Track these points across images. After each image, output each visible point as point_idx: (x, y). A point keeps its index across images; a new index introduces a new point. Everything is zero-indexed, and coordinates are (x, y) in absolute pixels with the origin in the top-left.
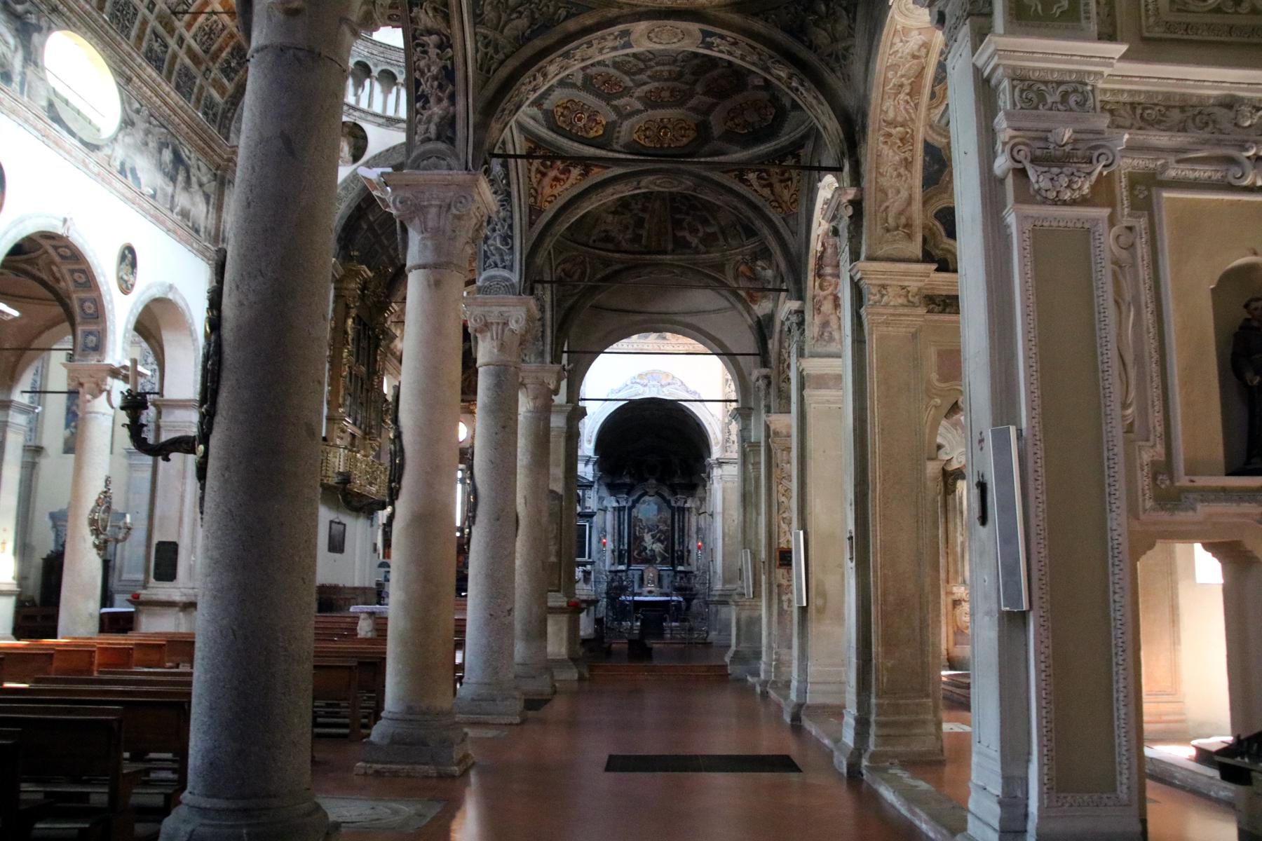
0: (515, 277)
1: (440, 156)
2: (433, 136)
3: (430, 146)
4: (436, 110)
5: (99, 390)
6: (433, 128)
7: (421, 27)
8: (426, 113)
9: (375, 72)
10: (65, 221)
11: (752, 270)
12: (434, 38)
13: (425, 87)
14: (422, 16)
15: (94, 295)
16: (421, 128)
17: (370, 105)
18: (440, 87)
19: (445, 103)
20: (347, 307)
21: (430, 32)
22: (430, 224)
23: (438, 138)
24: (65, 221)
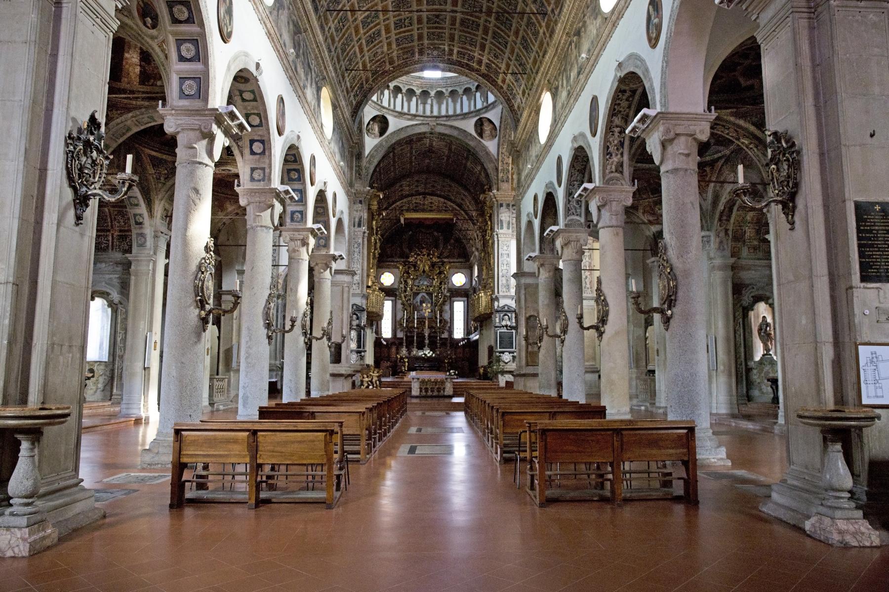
0: (582, 220)
1: (618, 179)
2: (614, 170)
3: (612, 175)
4: (615, 159)
5: (327, 266)
6: (614, 167)
7: (614, 124)
8: (611, 161)
9: (404, 91)
10: (325, 183)
11: (653, 210)
12: (619, 129)
13: (611, 149)
14: (616, 120)
15: (326, 219)
16: (609, 167)
17: (389, 105)
18: (617, 149)
19: (619, 156)
20: (373, 215)
21: (617, 126)
22: (614, 209)
23: (616, 171)
24: (325, 183)
